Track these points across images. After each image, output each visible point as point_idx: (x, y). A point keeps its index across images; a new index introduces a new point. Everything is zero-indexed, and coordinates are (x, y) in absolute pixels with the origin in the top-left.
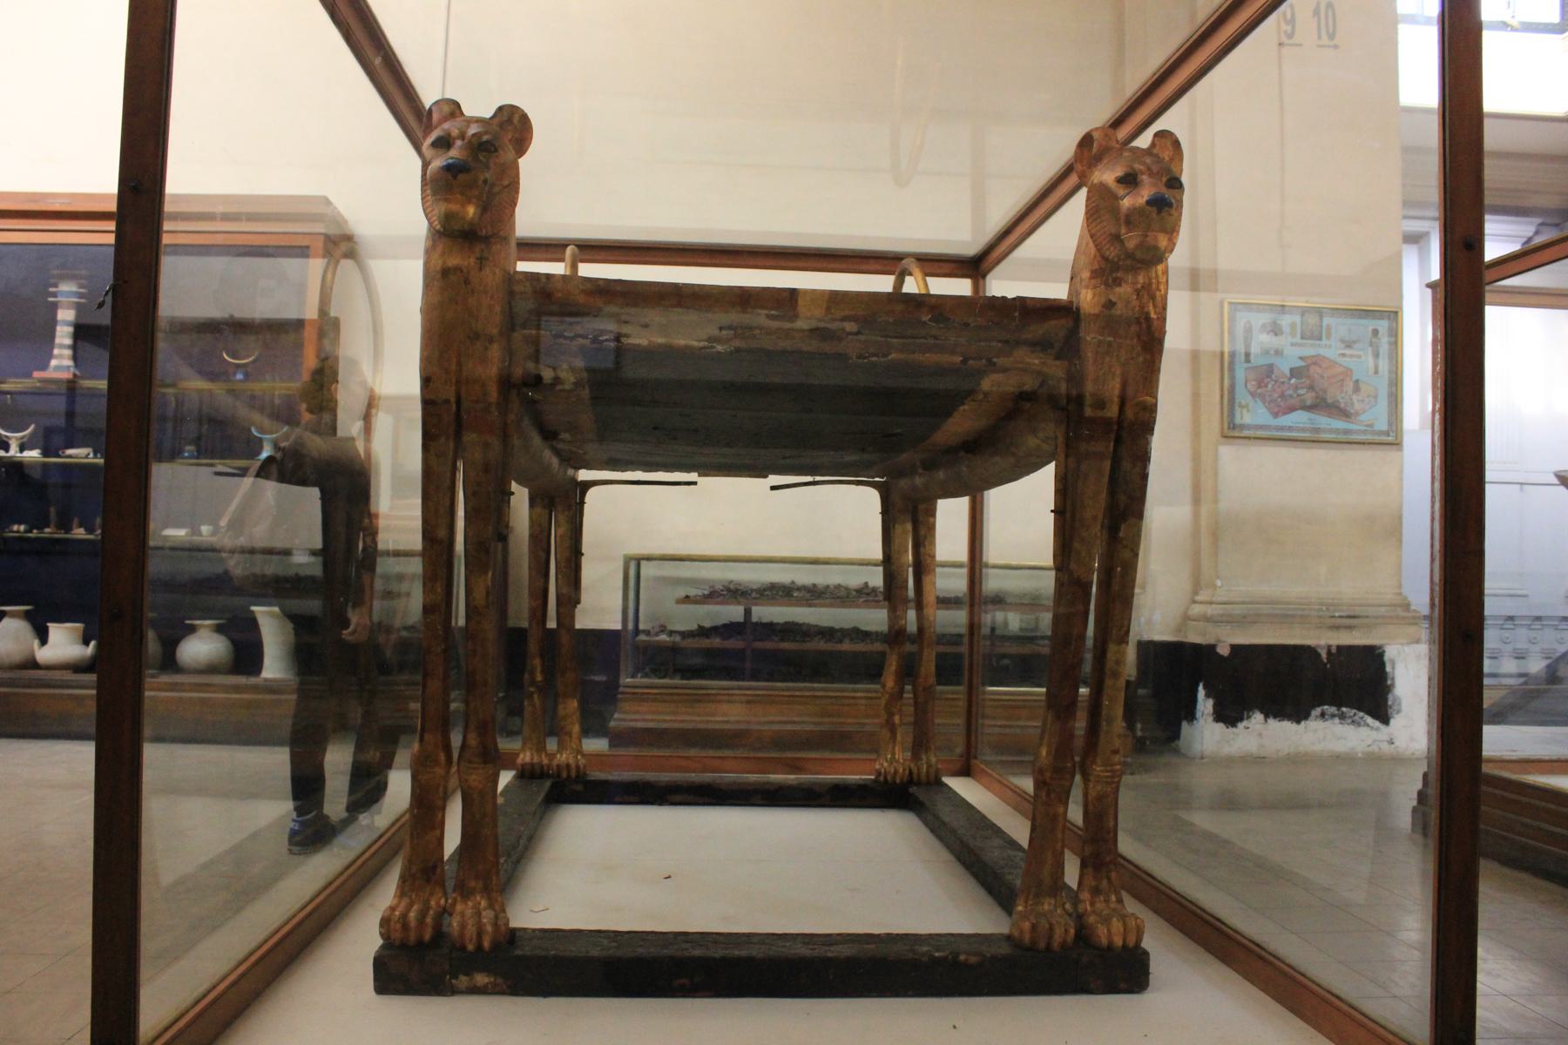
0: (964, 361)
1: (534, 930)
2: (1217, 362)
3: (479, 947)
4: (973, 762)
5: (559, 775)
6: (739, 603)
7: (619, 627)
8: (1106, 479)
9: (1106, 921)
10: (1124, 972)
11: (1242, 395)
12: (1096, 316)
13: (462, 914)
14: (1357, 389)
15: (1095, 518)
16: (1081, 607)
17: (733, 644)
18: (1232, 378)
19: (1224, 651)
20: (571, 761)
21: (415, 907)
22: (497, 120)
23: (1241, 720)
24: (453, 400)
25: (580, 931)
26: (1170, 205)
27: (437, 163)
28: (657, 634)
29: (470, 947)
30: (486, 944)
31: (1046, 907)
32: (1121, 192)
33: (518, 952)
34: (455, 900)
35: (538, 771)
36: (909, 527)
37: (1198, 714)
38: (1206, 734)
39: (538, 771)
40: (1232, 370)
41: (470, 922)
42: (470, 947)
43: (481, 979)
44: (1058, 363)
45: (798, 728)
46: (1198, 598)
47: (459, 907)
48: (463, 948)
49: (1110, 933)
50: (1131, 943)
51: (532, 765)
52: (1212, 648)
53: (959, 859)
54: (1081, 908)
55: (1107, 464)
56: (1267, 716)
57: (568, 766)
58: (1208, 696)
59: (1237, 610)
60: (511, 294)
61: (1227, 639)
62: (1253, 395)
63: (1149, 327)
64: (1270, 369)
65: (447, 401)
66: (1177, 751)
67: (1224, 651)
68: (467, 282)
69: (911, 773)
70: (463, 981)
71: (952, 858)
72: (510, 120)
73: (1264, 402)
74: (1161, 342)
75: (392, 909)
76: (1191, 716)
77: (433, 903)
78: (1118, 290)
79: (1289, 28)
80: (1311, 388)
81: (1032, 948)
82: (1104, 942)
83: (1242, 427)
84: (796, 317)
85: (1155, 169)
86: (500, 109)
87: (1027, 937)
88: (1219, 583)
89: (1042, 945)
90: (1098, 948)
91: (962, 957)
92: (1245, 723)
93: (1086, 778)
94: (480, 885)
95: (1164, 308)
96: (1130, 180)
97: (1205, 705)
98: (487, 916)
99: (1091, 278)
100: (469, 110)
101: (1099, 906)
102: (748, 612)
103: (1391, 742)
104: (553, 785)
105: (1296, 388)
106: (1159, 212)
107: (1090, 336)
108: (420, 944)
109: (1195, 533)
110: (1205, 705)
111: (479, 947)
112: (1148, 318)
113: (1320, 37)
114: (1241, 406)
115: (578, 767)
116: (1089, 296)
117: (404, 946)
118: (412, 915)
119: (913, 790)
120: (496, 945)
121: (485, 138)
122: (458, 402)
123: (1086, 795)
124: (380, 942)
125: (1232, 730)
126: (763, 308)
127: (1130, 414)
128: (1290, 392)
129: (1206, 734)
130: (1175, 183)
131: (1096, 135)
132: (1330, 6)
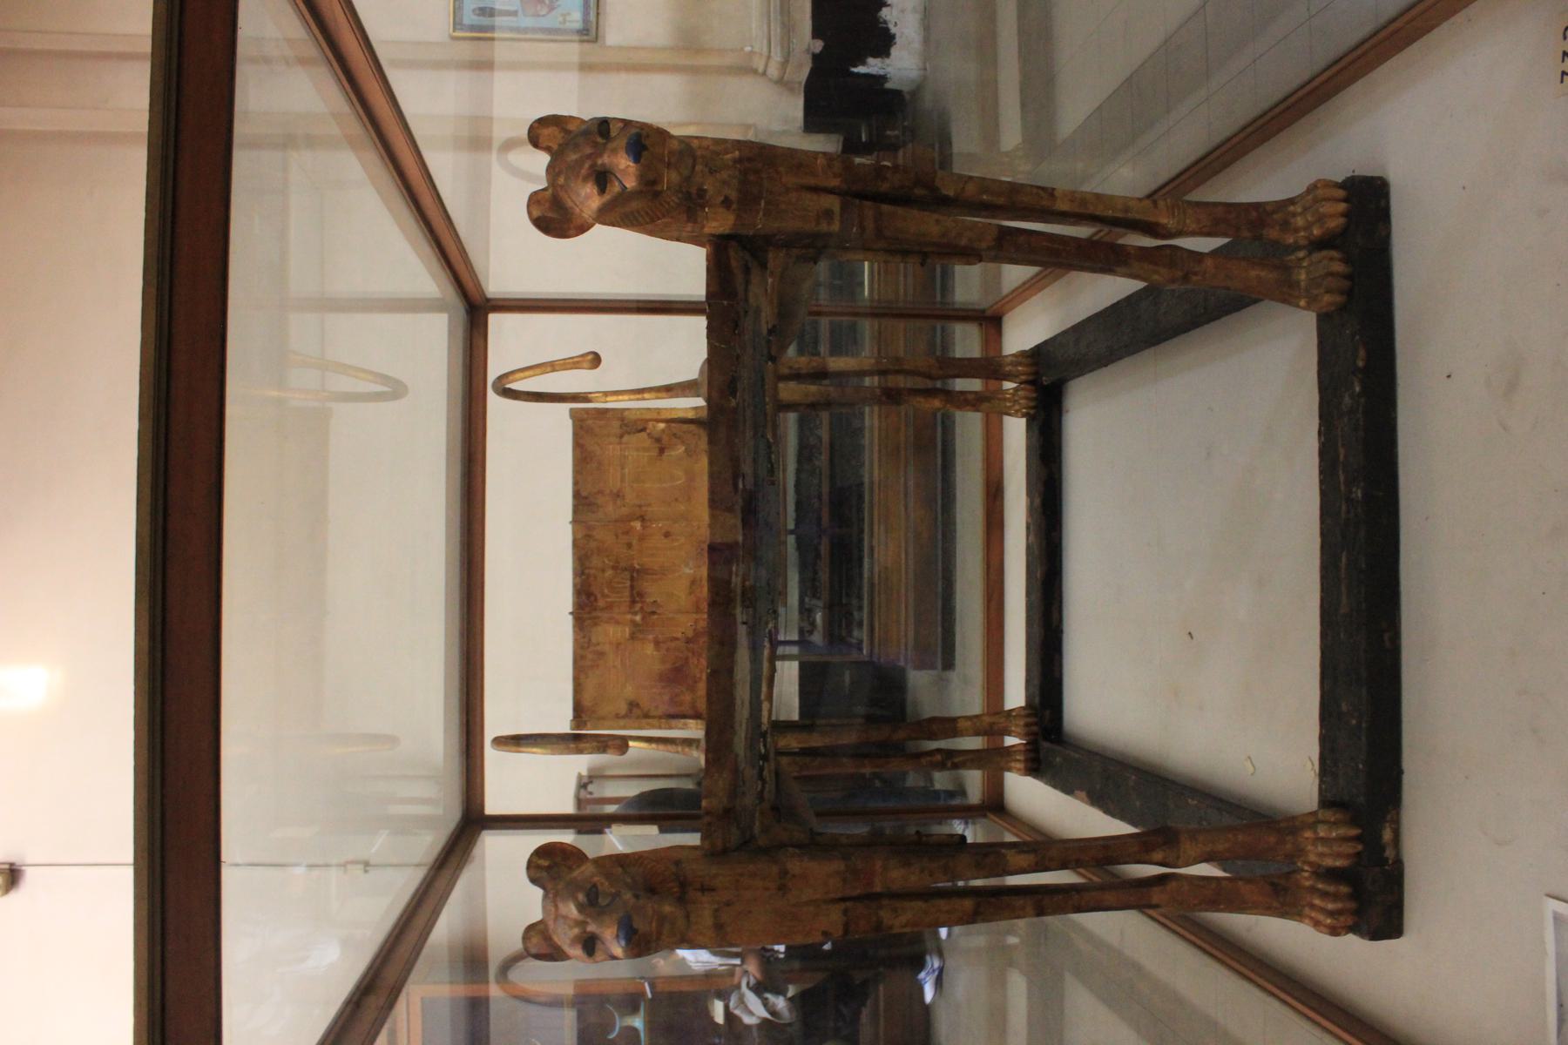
0: (773, 359)
1: (1321, 782)
2: (516, 44)
3: (1357, 839)
4: (989, 313)
5: (1035, 734)
6: (785, 543)
7: (795, 664)
8: (900, 211)
9: (1321, 219)
10: (1368, 200)
12: (738, 217)
13: (1322, 855)
15: (938, 221)
16: (1022, 239)
17: (824, 549)
18: (534, 30)
19: (818, 46)
20: (1022, 723)
21: (1317, 902)
22: (549, 886)
23: (888, 29)
24: (843, 906)
25: (1323, 739)
26: (639, 136)
27: (618, 950)
28: (813, 624)
29: (1360, 847)
30: (1354, 832)
31: (1303, 277)
32: (615, 188)
33: (1362, 799)
34: (1304, 862)
35: (1032, 755)
36: (781, 385)
37: (882, 72)
38: (900, 65)
39: (1032, 755)
40: (526, 30)
41: (1335, 848)
42: (1360, 847)
43: (1387, 835)
44: (770, 255)
45: (911, 483)
46: (761, 70)
47: (1312, 858)
48: (1358, 854)
49: (1334, 213)
50: (1341, 193)
51: (1026, 761)
52: (816, 58)
53: (1154, 344)
54: (1303, 242)
55: (885, 208)
56: (885, 5)
57: (1027, 725)
58: (864, 63)
59: (777, 30)
60: (725, 851)
61: (806, 41)
62: (551, 9)
63: (750, 160)
65: (845, 912)
66: (917, 91)
67: (818, 46)
68: (728, 904)
69: (1025, 382)
70: (1389, 853)
71: (1152, 350)
72: (549, 868)
74: (738, 141)
75: (1317, 924)
76: (882, 79)
77: (1307, 883)
78: (711, 192)
81: (1349, 293)
82: (1342, 220)
83: (586, 20)
84: (737, 543)
85: (588, 150)
86: (534, 881)
87: (1338, 299)
88: (748, 49)
89: (1347, 284)
90: (1345, 231)
91: (1360, 364)
92: (891, 26)
93: (1179, 234)
94: (1289, 838)
95: (725, 141)
96: (602, 178)
97: (873, 66)
98: (1322, 832)
99: (695, 222)
100: (537, 915)
101: (1300, 221)
102: (792, 532)
104: (1046, 739)
106: (644, 148)
107: (760, 223)
108: (1356, 895)
109: (694, 70)
110: (873, 66)
111: (1357, 839)
112: (739, 161)
115: (1028, 716)
116: (714, 224)
117: (1358, 913)
118: (1330, 906)
119: (1046, 380)
120: (1353, 822)
121: (581, 897)
122: (843, 899)
123: (1193, 234)
124: (1351, 937)
125: (897, 40)
126: (729, 582)
127: (834, 183)
129: (900, 65)
130: (603, 126)
131: (536, 213)
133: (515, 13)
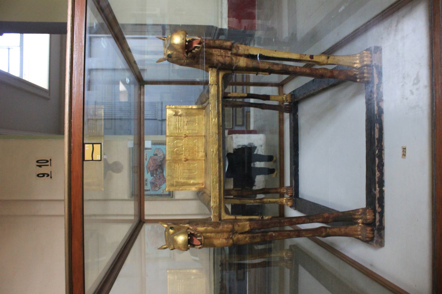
11: (160, 192)
14: (156, 155)
62: (159, 189)
64: (152, 183)
73: (161, 185)
79: (46, 175)
80: (156, 170)
103: (261, 146)
105: (157, 175)
113: (48, 165)
114: (163, 192)
128: (158, 176)
132: (37, 162)
133: (149, 190)
